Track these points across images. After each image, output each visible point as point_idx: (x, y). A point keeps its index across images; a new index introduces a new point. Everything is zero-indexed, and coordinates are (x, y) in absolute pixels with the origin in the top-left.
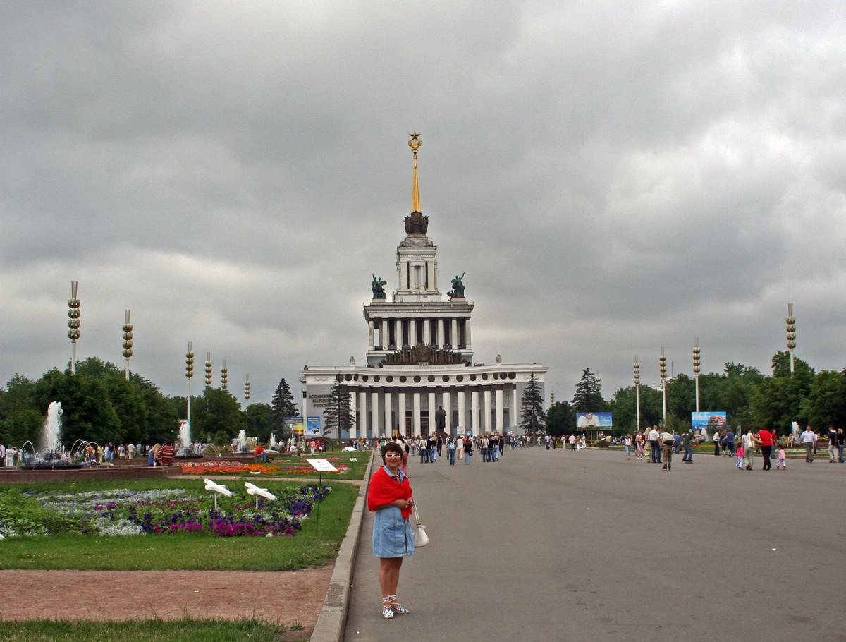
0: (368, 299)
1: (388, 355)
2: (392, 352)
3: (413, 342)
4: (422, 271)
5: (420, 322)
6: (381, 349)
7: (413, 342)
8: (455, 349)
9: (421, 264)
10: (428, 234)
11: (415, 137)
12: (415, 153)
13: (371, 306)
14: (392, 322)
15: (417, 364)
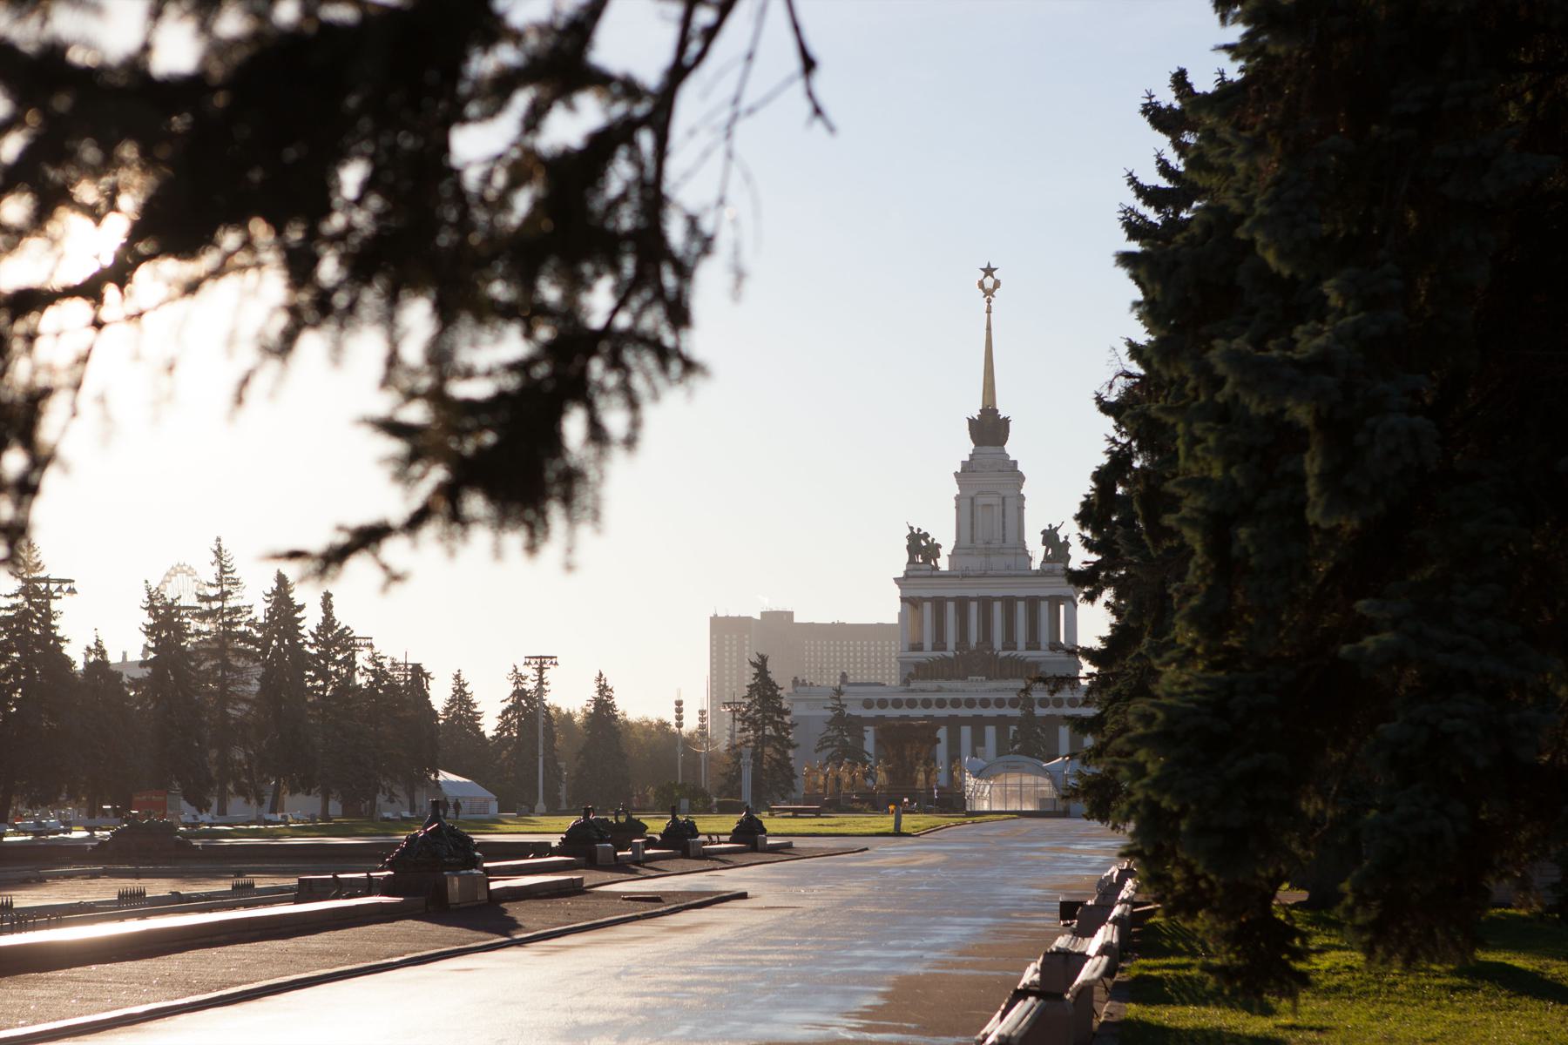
0: (899, 562)
1: (918, 666)
2: (938, 654)
3: (973, 639)
4: (997, 511)
5: (986, 603)
6: (921, 649)
7: (973, 639)
8: (1042, 654)
9: (995, 500)
10: (1010, 448)
11: (989, 271)
12: (989, 301)
13: (907, 576)
14: (939, 604)
15: (964, 678)
